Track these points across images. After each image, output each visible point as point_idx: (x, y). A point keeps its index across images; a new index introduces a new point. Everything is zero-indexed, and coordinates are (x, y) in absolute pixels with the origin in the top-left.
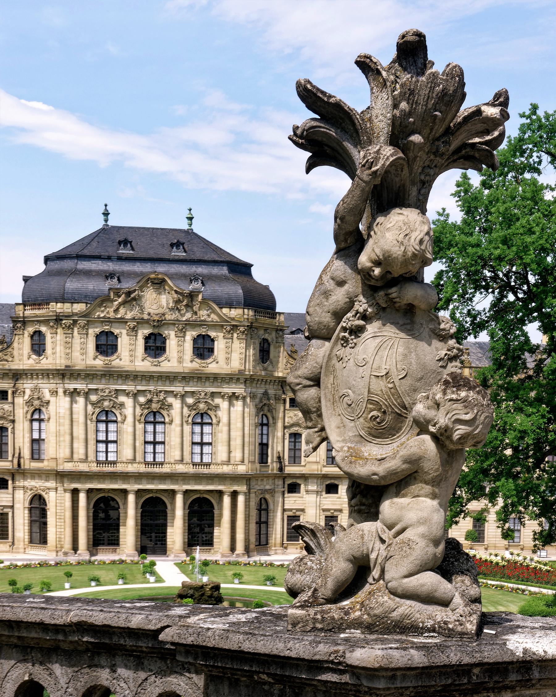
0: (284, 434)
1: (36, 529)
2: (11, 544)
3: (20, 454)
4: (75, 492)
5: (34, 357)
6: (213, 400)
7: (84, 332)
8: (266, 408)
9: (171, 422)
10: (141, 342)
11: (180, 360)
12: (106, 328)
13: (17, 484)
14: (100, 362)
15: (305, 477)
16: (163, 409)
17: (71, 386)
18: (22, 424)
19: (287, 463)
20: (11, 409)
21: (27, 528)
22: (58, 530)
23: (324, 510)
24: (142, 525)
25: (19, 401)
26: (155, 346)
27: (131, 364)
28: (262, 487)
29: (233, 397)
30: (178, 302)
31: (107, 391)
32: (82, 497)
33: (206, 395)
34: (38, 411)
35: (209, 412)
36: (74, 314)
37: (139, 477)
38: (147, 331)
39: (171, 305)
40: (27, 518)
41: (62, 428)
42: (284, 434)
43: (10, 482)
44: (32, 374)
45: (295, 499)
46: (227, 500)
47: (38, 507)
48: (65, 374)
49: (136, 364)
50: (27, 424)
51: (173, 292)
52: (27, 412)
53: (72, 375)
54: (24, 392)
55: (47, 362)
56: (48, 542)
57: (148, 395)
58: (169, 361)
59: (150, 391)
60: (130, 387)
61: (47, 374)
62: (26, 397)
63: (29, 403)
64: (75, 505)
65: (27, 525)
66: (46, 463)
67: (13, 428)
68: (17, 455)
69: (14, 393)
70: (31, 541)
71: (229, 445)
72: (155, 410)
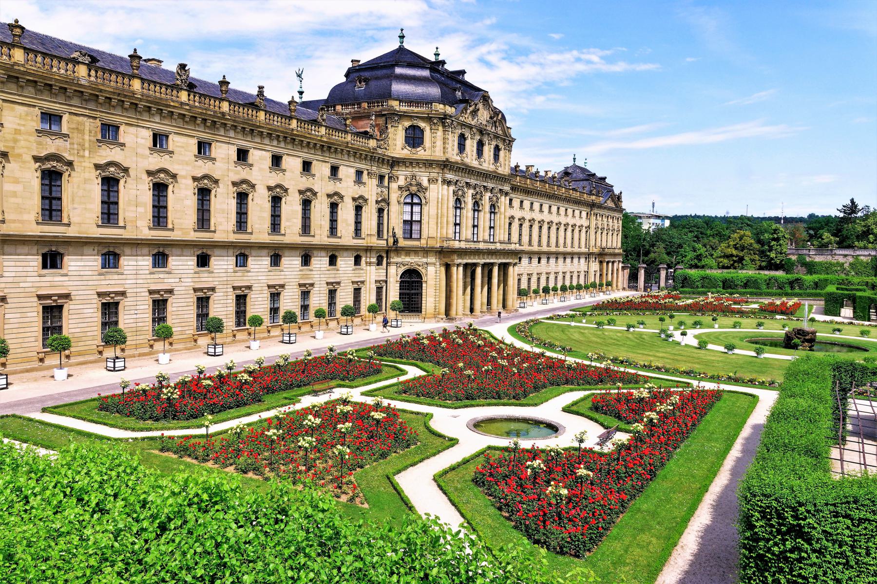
13: (392, 260)
14: (458, 158)
17: (450, 176)
20: (387, 193)
25: (394, 186)
29: (507, 194)
30: (491, 118)
47: (412, 282)
48: (446, 165)
55: (426, 153)
60: (473, 182)
61: (429, 164)
62: (402, 182)
66: (423, 242)
68: (391, 234)
69: (390, 178)
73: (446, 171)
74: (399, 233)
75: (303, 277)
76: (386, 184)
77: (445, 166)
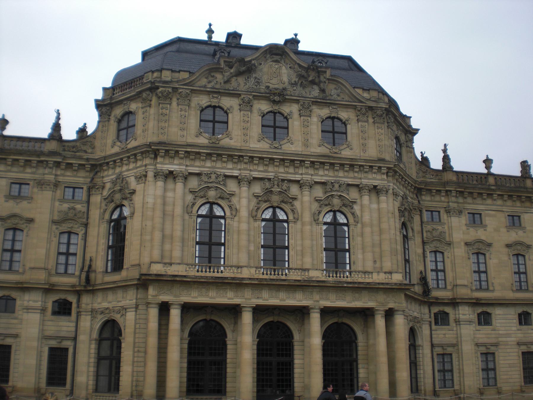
0: (424, 251)
1: (104, 371)
2: (68, 392)
3: (90, 266)
4: (164, 309)
5: (119, 144)
6: (348, 194)
7: (186, 103)
8: (406, 214)
9: (296, 220)
10: (256, 120)
11: (306, 144)
12: (215, 102)
14: (203, 140)
15: (454, 303)
16: (286, 203)
18: (97, 229)
20: (85, 209)
21: (92, 369)
22: (135, 369)
23: (477, 345)
24: (258, 363)
25: (96, 199)
26: (275, 126)
27: (243, 144)
30: (301, 76)
31: (213, 176)
32: (175, 314)
33: (339, 186)
34: (118, 209)
35: (344, 209)
36: (171, 82)
37: (258, 285)
39: (294, 79)
40: (93, 355)
41: (149, 223)
42: (424, 251)
43: (74, 306)
44: (115, 161)
45: (444, 332)
49: (251, 146)
50: (104, 227)
51: (296, 66)
52: (105, 211)
53: (167, 151)
54: (103, 188)
56: (120, 387)
57: (267, 184)
58: (292, 144)
59: (269, 179)
62: (105, 193)
63: (109, 199)
64: (163, 332)
65: (92, 365)
66: (124, 273)
67: (86, 234)
68: (86, 269)
69: (89, 189)
70: (96, 390)
71: (373, 252)
72: (275, 204)
73: (159, 160)
74: (99, 265)
76: (85, 198)
77: (156, 154)
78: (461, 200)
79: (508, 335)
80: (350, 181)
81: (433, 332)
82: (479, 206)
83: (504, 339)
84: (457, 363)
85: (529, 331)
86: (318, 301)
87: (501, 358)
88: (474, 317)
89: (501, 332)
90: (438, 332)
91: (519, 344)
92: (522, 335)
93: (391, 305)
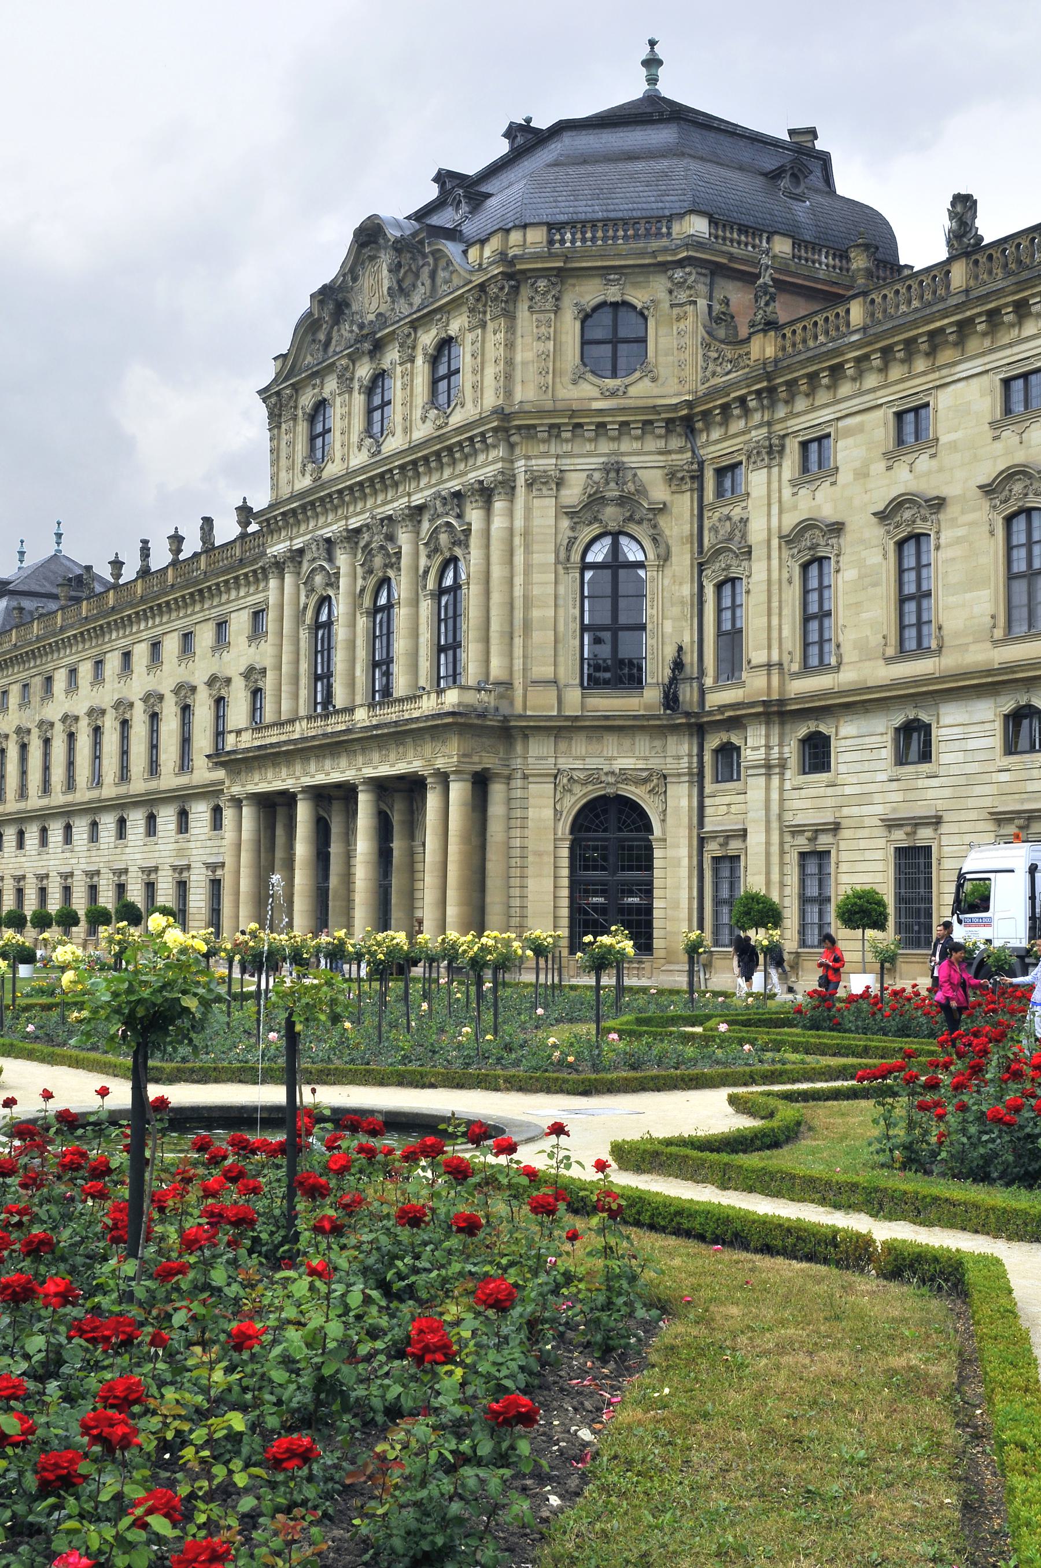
19: (709, 681)
23: (797, 831)
28: (592, 763)
38: (364, 371)
42: (701, 587)
45: (727, 800)
46: (432, 800)
75: (180, 852)
78: (781, 412)
79: (864, 799)
80: (455, 485)
81: (707, 802)
82: (805, 417)
83: (855, 811)
84: (788, 880)
85: (920, 783)
86: (360, 769)
87: (843, 867)
88: (791, 751)
89: (848, 790)
90: (717, 800)
91: (891, 824)
92: (898, 797)
93: (440, 763)
